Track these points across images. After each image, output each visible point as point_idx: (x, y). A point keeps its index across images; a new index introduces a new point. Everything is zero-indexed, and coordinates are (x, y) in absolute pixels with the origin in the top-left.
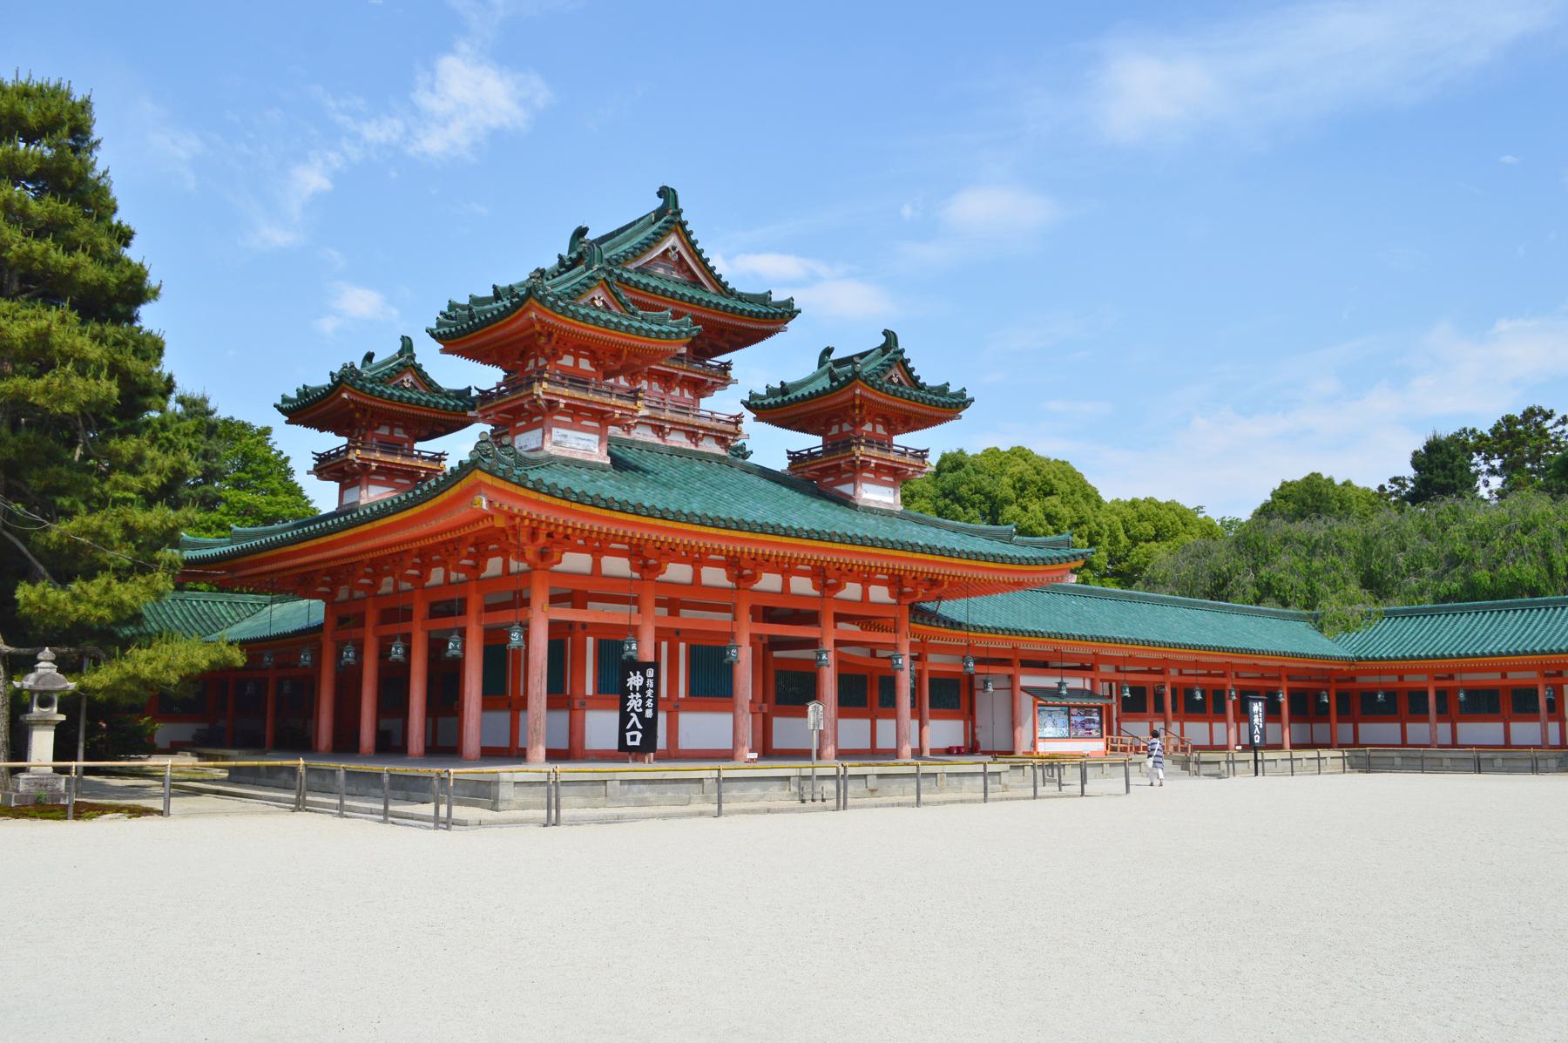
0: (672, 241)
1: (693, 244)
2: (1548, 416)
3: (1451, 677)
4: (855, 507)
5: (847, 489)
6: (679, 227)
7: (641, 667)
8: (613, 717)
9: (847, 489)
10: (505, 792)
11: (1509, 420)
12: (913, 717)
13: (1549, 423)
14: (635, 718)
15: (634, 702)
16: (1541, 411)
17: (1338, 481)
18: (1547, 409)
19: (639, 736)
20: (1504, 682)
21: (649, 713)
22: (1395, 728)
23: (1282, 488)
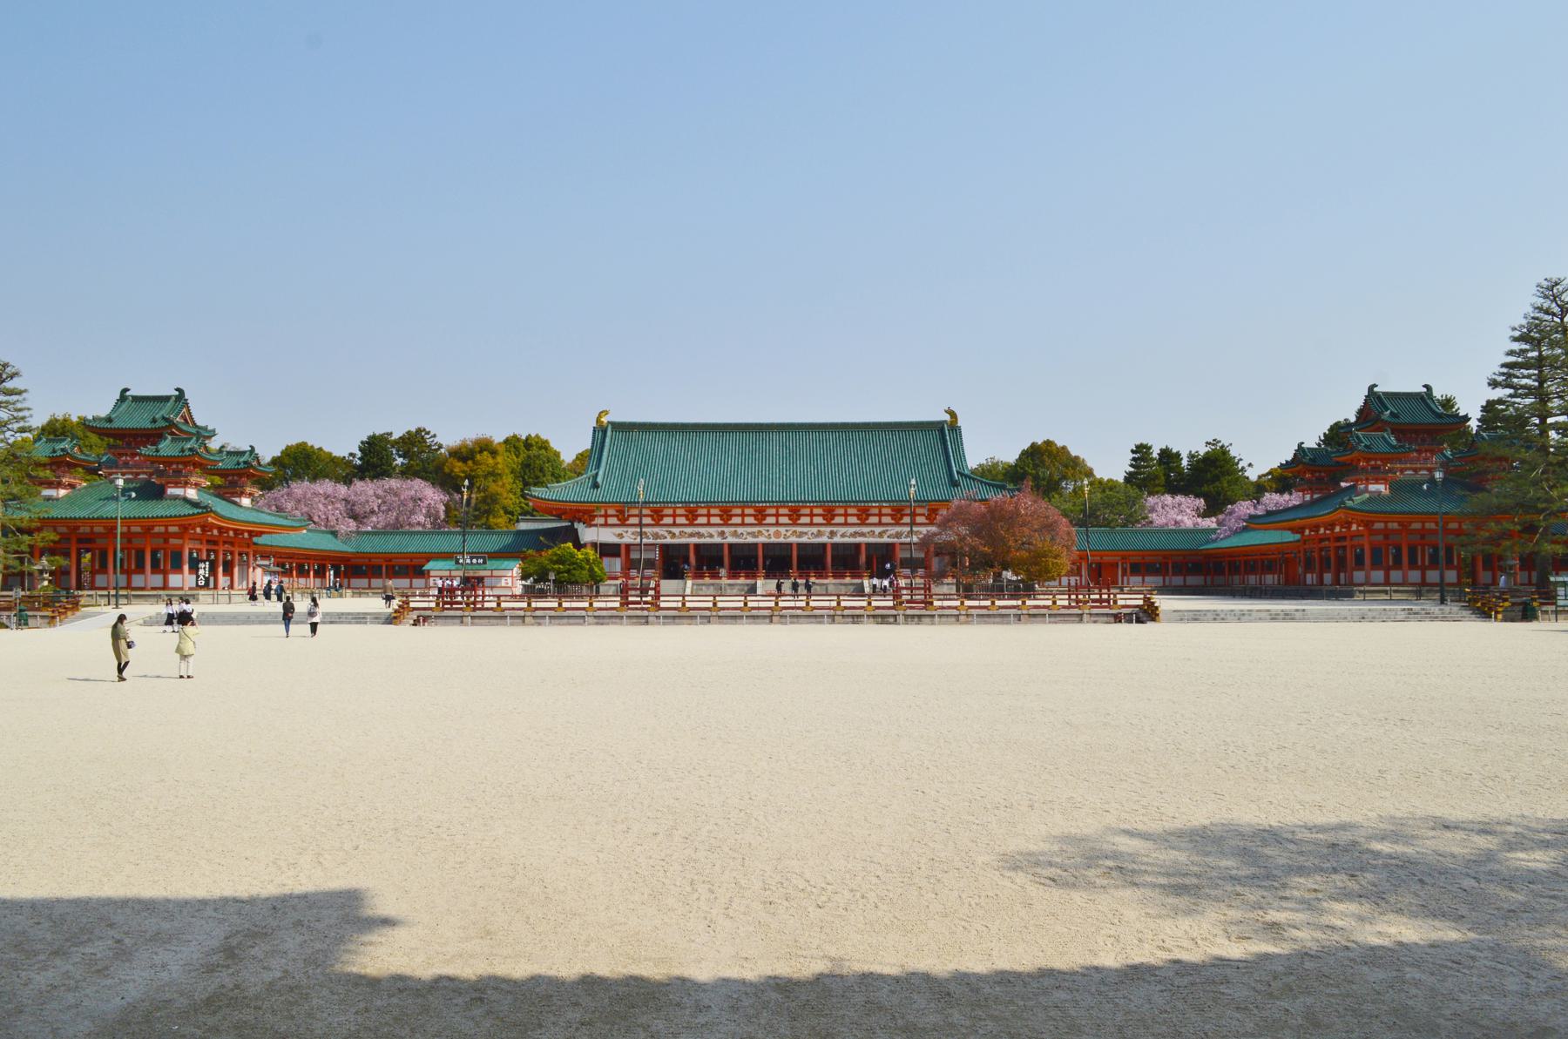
0: (184, 410)
1: (189, 410)
2: (428, 433)
3: (390, 560)
4: (241, 506)
5: (237, 500)
6: (186, 404)
7: (204, 562)
8: (195, 576)
9: (237, 500)
10: (200, 597)
11: (409, 432)
12: (224, 575)
13: (427, 436)
14: (202, 577)
15: (201, 572)
16: (424, 430)
17: (310, 444)
18: (427, 430)
19: (203, 582)
20: (413, 563)
21: (207, 575)
22: (366, 581)
23: (286, 449)
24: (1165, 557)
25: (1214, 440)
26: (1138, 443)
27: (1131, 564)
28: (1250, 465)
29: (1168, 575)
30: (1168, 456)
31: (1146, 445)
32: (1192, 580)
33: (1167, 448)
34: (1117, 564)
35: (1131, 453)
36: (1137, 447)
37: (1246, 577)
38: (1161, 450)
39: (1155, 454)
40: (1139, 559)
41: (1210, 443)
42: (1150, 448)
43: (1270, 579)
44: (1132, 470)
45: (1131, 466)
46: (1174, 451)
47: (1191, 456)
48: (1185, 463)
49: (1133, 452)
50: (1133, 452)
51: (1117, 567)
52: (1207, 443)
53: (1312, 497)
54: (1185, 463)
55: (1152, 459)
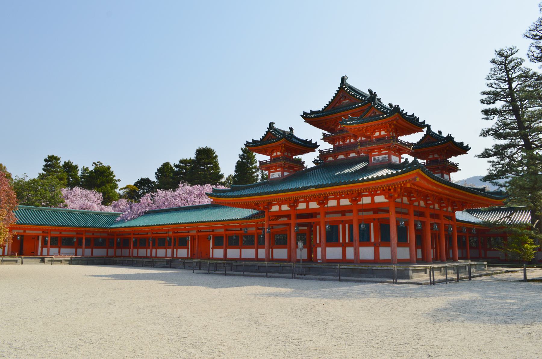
24: (78, 233)
25: (98, 162)
26: (51, 155)
27: (52, 238)
28: (119, 180)
29: (81, 247)
30: (70, 167)
31: (56, 157)
32: (99, 252)
33: (69, 162)
34: (38, 237)
35: (44, 161)
36: (49, 157)
37: (175, 250)
38: (65, 162)
39: (62, 163)
40: (57, 233)
41: (95, 164)
42: (59, 159)
43: (183, 253)
44: (44, 173)
45: (44, 170)
46: (74, 164)
47: (85, 170)
48: (80, 173)
49: (46, 160)
50: (46, 160)
51: (38, 239)
52: (94, 163)
53: (283, 174)
54: (80, 173)
55: (59, 167)
